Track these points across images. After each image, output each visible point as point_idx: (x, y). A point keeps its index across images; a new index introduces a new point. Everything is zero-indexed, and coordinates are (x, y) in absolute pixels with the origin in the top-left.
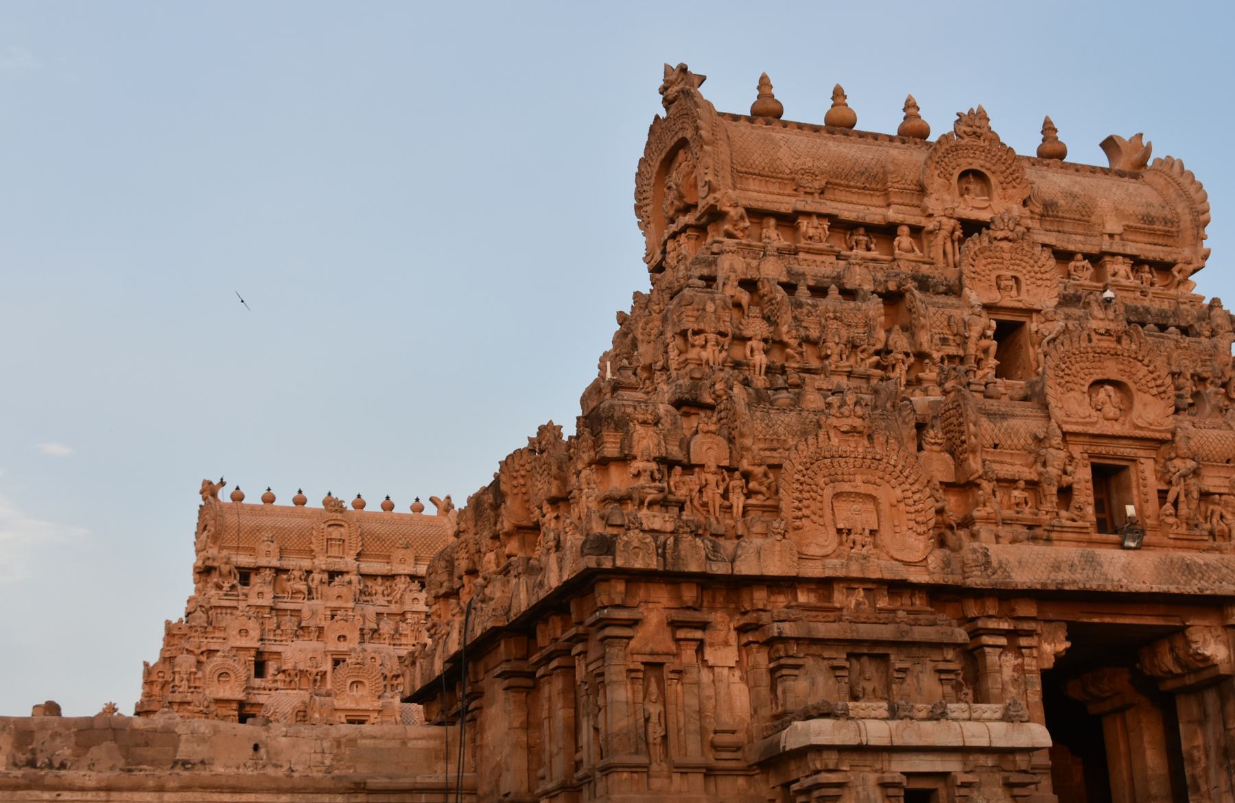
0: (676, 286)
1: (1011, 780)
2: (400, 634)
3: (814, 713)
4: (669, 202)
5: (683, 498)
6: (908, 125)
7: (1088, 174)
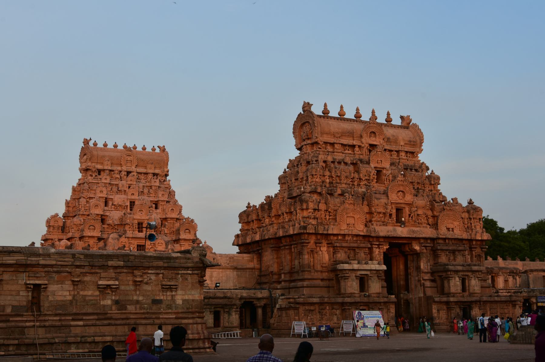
2: (150, 193)
6: (357, 115)
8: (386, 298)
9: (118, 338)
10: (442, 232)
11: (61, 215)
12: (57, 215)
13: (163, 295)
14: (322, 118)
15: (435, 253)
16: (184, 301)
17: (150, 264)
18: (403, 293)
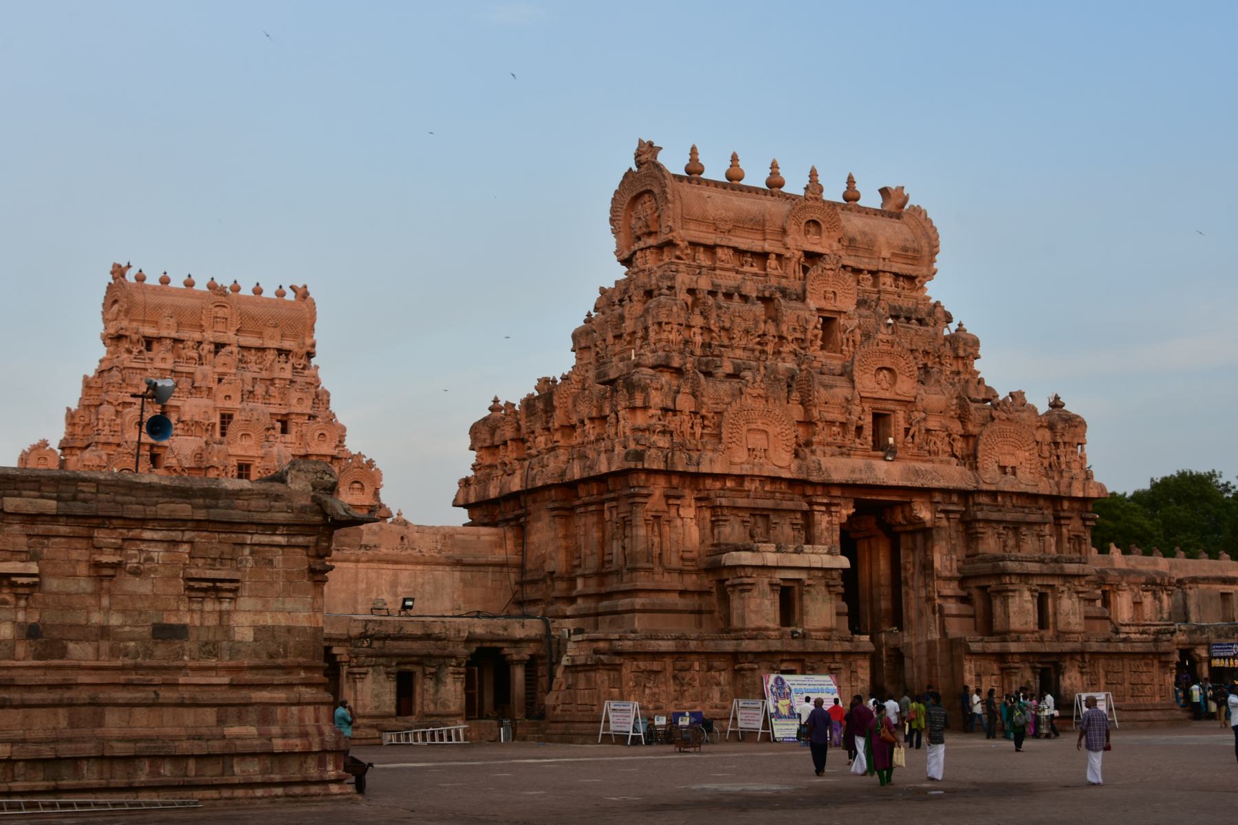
6: (773, 180)
9: (32, 747)
11: (54, 444)
12: (44, 444)
13: (191, 611)
14: (685, 183)
15: (969, 529)
16: (259, 630)
17: (148, 509)
18: (885, 632)
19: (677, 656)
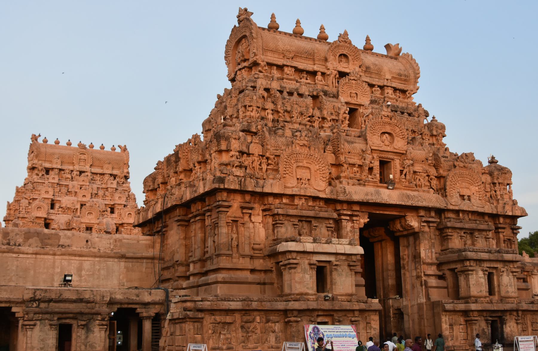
0: (241, 89)
1: (350, 264)
3: (289, 240)
4: (238, 57)
5: (247, 165)
6: (321, 35)
7: (381, 57)
8: (364, 303)
10: (453, 201)
14: (266, 31)
18: (392, 299)
19: (243, 312)
